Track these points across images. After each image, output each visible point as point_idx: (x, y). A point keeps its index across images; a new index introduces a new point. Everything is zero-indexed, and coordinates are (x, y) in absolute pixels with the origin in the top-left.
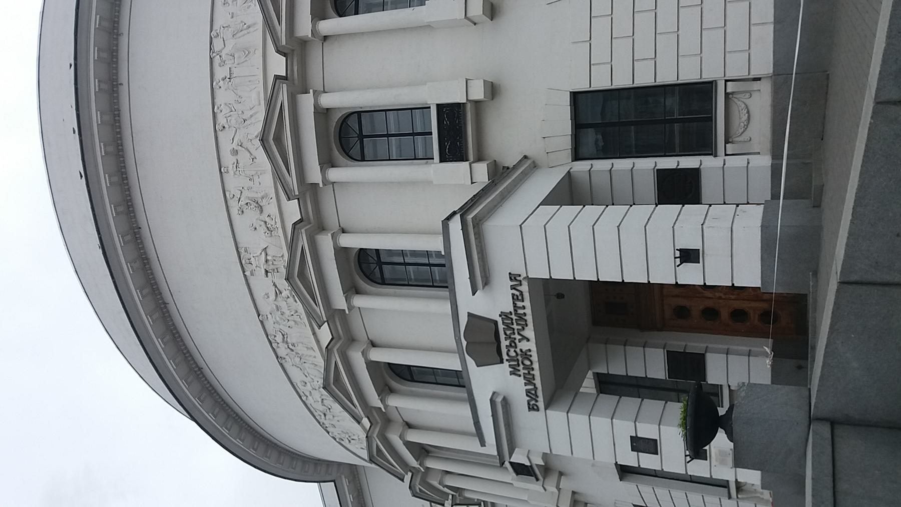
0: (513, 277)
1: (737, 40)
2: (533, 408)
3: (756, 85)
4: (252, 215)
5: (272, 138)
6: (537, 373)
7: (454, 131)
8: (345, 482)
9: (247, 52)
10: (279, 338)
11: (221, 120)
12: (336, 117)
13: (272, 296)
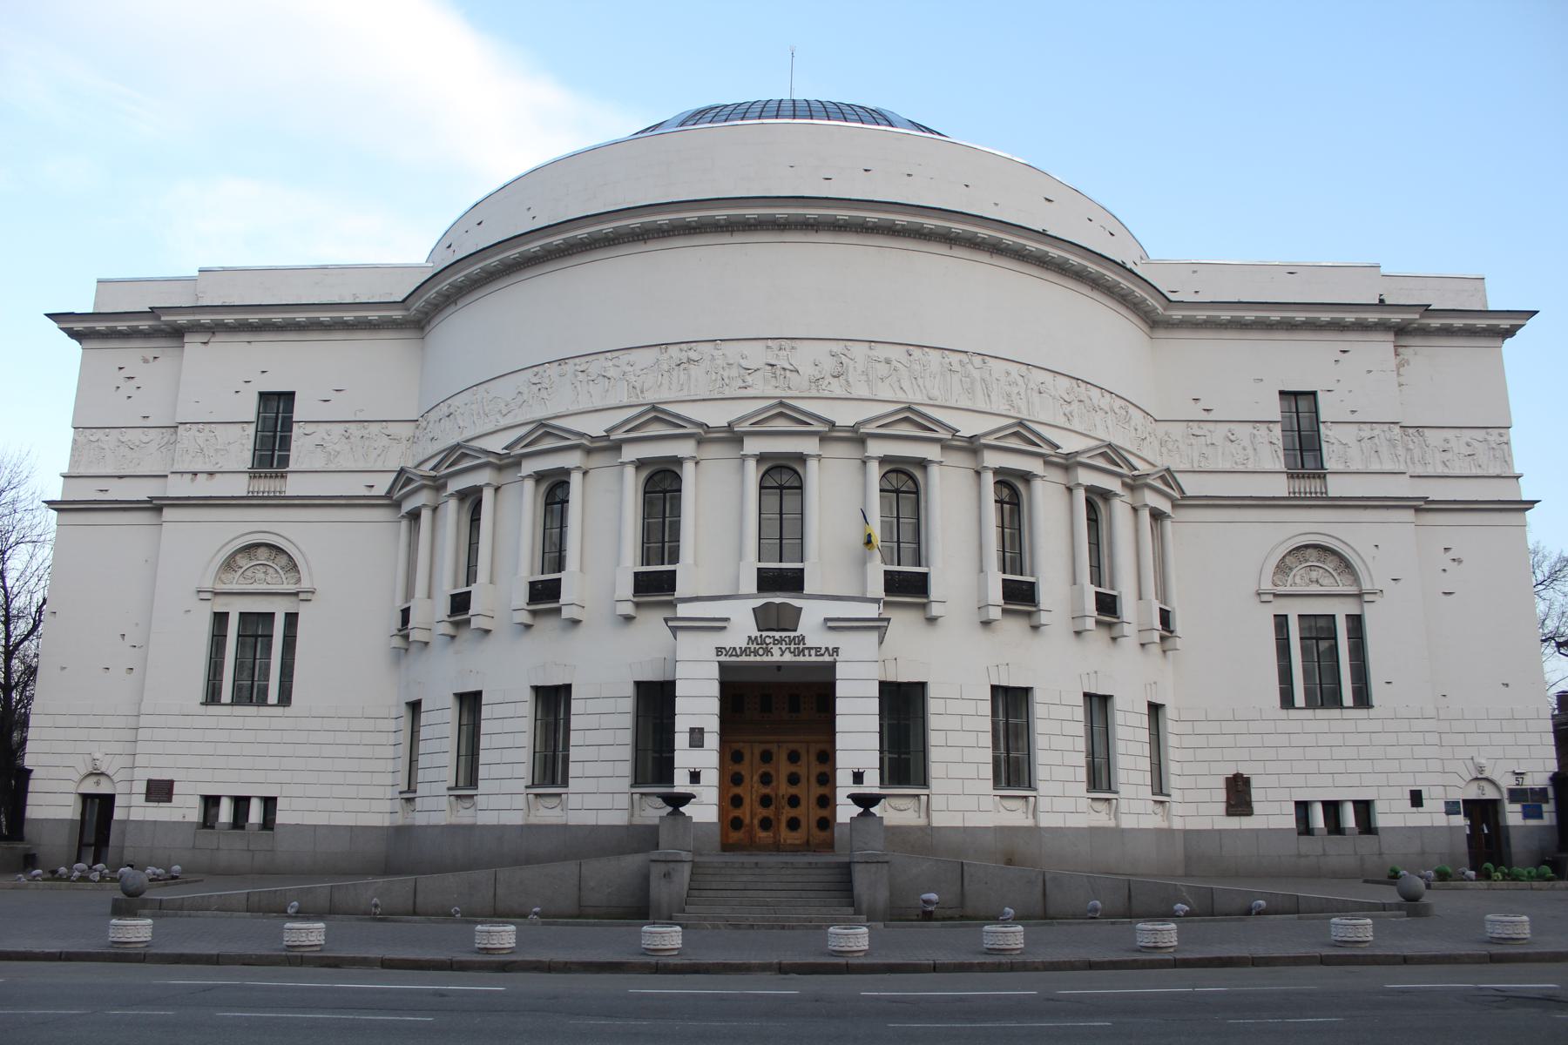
0: (836, 650)
2: (719, 650)
3: (923, 814)
4: (829, 365)
5: (910, 414)
6: (752, 658)
7: (908, 586)
8: (397, 314)
9: (970, 391)
10: (693, 355)
11: (917, 352)
12: (918, 474)
13: (745, 363)
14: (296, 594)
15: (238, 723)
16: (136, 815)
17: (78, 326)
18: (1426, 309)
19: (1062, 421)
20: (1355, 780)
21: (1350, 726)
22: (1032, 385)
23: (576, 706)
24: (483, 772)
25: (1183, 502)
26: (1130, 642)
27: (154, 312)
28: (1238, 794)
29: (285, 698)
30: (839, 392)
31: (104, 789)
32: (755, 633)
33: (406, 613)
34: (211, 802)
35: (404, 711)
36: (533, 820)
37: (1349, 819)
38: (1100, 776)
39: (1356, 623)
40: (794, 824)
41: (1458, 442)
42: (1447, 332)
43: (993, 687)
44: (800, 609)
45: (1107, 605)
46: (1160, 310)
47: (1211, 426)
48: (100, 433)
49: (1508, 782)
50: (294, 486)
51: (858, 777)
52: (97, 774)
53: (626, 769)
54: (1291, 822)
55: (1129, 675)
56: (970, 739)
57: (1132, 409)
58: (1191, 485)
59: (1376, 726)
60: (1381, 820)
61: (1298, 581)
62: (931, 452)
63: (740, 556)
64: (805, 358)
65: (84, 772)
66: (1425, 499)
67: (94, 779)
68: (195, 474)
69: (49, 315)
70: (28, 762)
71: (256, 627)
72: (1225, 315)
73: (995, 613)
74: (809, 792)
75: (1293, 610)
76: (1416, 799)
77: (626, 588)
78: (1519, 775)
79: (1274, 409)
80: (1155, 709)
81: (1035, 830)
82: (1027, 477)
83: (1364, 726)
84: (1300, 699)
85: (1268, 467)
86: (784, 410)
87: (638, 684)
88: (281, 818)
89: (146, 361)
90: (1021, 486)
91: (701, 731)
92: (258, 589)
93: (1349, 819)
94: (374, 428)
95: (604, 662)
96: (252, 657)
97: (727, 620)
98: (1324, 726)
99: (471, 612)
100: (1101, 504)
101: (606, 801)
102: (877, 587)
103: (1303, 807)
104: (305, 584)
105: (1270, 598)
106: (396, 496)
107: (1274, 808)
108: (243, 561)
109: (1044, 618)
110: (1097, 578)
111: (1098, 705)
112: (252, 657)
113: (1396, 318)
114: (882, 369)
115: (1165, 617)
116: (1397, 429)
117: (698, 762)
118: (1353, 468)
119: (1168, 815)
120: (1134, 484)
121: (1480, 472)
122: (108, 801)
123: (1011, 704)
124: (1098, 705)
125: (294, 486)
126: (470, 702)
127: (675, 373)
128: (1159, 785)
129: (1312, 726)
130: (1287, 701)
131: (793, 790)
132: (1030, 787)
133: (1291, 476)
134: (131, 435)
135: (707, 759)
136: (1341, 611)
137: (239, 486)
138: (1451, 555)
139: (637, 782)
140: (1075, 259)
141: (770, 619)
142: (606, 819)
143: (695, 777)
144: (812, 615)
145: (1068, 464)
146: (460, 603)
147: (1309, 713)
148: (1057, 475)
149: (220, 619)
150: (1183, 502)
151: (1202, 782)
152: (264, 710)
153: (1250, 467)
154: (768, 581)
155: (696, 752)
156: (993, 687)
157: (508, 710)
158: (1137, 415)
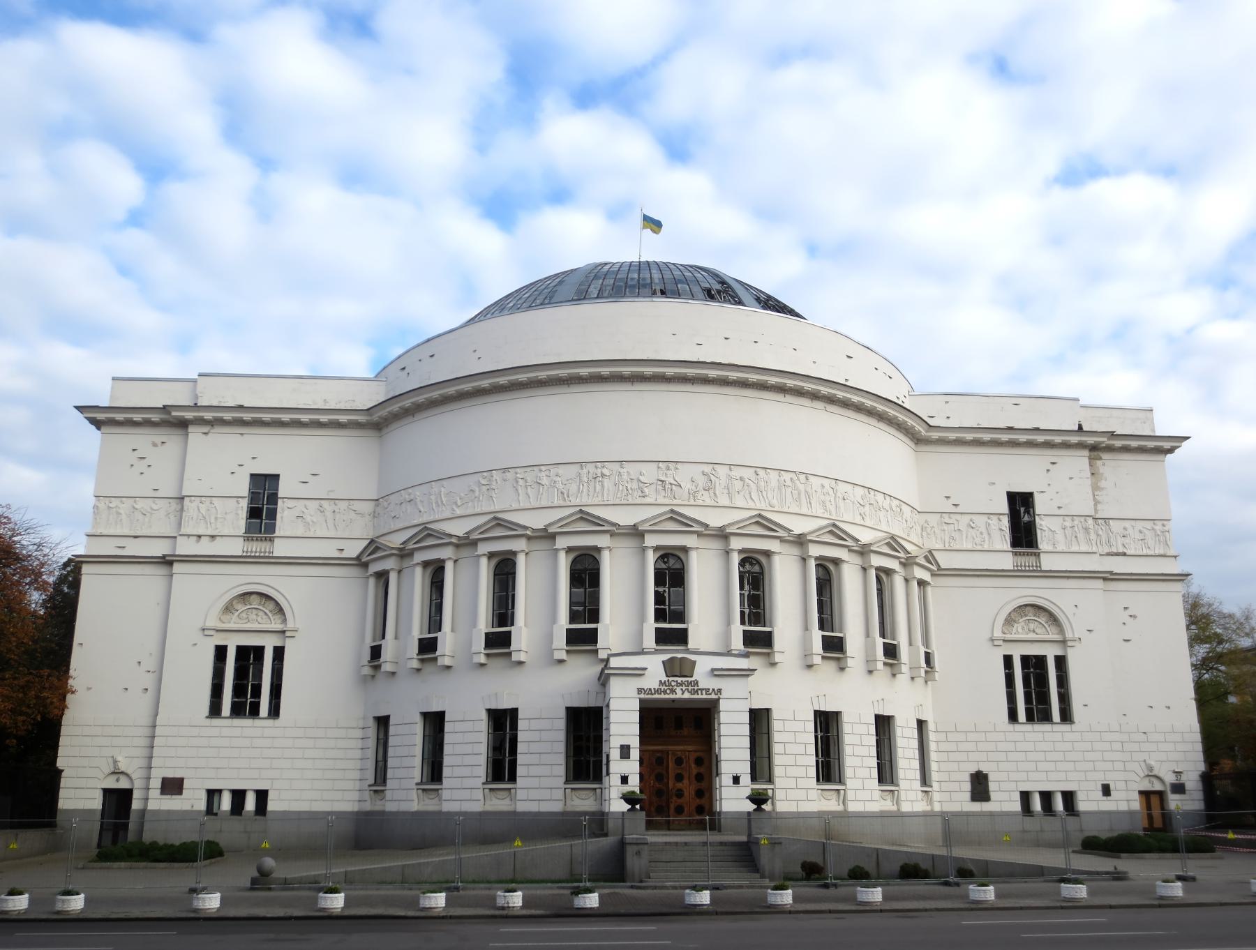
0: (720, 691)
1: (793, 794)
2: (640, 690)
4: (702, 481)
6: (662, 696)
7: (759, 641)
8: (361, 418)
9: (798, 500)
10: (606, 471)
11: (761, 472)
13: (642, 478)
14: (284, 632)
15: (237, 732)
16: (152, 805)
17: (101, 416)
18: (1112, 435)
19: (858, 520)
20: (1062, 776)
21: (1058, 737)
22: (839, 494)
23: (521, 725)
24: (446, 772)
25: (939, 572)
26: (903, 678)
27: (165, 409)
28: (980, 786)
29: (275, 711)
30: (709, 502)
31: (123, 784)
32: (664, 678)
33: (376, 652)
34: (213, 794)
35: (371, 723)
36: (489, 808)
37: (1059, 805)
38: (886, 773)
39: (1061, 662)
40: (679, 810)
41: (1133, 530)
42: (1126, 449)
43: (816, 712)
44: (694, 662)
45: (891, 651)
46: (923, 433)
47: (958, 517)
48: (115, 502)
49: (1170, 778)
50: (280, 548)
51: (736, 780)
52: (117, 773)
53: (561, 770)
54: (1017, 806)
55: (905, 700)
56: (801, 749)
57: (904, 507)
58: (945, 561)
59: (1077, 736)
60: (1082, 805)
61: (1019, 631)
62: (772, 546)
63: (642, 619)
64: (684, 475)
65: (107, 771)
66: (1111, 573)
67: (115, 777)
68: (199, 537)
69: (77, 408)
70: (60, 763)
71: (249, 657)
72: (969, 436)
73: (817, 660)
74: (688, 787)
75: (1017, 653)
76: (1106, 790)
77: (560, 640)
78: (1178, 773)
79: (1004, 507)
80: (921, 724)
81: (845, 815)
82: (837, 562)
83: (1069, 737)
84: (1022, 715)
85: (999, 547)
86: (674, 516)
87: (567, 709)
88: (271, 806)
89: (155, 445)
90: (831, 567)
91: (628, 747)
92: (252, 628)
93: (1059, 805)
94: (343, 505)
95: (541, 691)
96: (246, 682)
97: (645, 669)
98: (1039, 736)
99: (438, 653)
100: (884, 576)
101: (546, 794)
102: (738, 643)
103: (1025, 797)
104: (290, 625)
105: (1001, 643)
106: (365, 559)
107: (1005, 796)
108: (241, 607)
109: (850, 662)
110: (883, 635)
111: (884, 724)
112: (246, 682)
113: (1091, 440)
114: (738, 485)
115: (928, 658)
116: (1090, 521)
117: (624, 770)
118: (1059, 549)
119: (931, 802)
120: (908, 563)
121: (1150, 553)
122: (127, 794)
123: (827, 725)
124: (884, 724)
125: (280, 548)
126: (435, 722)
127: (592, 484)
128: (925, 780)
129: (1030, 736)
130: (1013, 716)
131: (679, 785)
132: (841, 782)
133: (1015, 554)
134: (140, 504)
135: (632, 767)
136: (1050, 652)
137: (236, 547)
138: (1129, 612)
139: (567, 781)
140: (868, 403)
141: (672, 668)
142: (546, 807)
143: (624, 780)
144: (703, 666)
145: (864, 551)
146: (428, 646)
147: (1029, 727)
148: (857, 560)
149: (221, 652)
150: (939, 572)
151: (955, 776)
152: (257, 722)
153: (986, 547)
154: (663, 637)
155: (625, 763)
156: (816, 712)
157: (468, 726)
158: (906, 509)
